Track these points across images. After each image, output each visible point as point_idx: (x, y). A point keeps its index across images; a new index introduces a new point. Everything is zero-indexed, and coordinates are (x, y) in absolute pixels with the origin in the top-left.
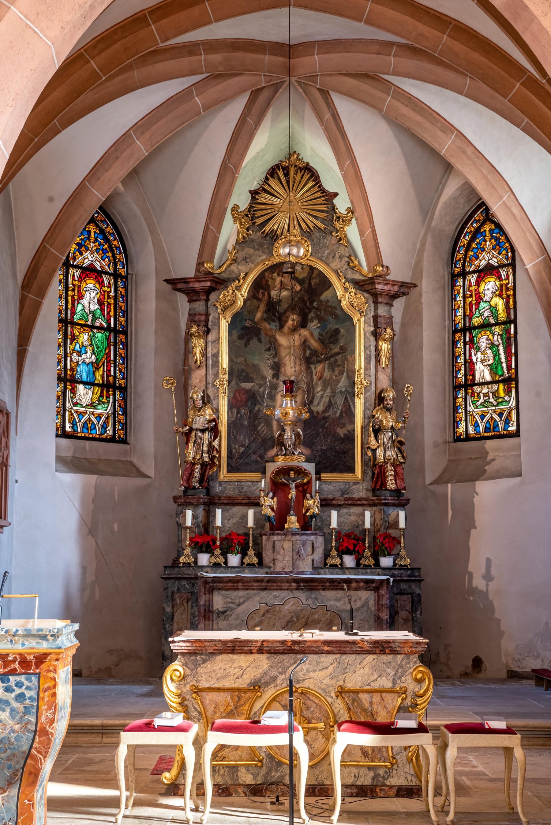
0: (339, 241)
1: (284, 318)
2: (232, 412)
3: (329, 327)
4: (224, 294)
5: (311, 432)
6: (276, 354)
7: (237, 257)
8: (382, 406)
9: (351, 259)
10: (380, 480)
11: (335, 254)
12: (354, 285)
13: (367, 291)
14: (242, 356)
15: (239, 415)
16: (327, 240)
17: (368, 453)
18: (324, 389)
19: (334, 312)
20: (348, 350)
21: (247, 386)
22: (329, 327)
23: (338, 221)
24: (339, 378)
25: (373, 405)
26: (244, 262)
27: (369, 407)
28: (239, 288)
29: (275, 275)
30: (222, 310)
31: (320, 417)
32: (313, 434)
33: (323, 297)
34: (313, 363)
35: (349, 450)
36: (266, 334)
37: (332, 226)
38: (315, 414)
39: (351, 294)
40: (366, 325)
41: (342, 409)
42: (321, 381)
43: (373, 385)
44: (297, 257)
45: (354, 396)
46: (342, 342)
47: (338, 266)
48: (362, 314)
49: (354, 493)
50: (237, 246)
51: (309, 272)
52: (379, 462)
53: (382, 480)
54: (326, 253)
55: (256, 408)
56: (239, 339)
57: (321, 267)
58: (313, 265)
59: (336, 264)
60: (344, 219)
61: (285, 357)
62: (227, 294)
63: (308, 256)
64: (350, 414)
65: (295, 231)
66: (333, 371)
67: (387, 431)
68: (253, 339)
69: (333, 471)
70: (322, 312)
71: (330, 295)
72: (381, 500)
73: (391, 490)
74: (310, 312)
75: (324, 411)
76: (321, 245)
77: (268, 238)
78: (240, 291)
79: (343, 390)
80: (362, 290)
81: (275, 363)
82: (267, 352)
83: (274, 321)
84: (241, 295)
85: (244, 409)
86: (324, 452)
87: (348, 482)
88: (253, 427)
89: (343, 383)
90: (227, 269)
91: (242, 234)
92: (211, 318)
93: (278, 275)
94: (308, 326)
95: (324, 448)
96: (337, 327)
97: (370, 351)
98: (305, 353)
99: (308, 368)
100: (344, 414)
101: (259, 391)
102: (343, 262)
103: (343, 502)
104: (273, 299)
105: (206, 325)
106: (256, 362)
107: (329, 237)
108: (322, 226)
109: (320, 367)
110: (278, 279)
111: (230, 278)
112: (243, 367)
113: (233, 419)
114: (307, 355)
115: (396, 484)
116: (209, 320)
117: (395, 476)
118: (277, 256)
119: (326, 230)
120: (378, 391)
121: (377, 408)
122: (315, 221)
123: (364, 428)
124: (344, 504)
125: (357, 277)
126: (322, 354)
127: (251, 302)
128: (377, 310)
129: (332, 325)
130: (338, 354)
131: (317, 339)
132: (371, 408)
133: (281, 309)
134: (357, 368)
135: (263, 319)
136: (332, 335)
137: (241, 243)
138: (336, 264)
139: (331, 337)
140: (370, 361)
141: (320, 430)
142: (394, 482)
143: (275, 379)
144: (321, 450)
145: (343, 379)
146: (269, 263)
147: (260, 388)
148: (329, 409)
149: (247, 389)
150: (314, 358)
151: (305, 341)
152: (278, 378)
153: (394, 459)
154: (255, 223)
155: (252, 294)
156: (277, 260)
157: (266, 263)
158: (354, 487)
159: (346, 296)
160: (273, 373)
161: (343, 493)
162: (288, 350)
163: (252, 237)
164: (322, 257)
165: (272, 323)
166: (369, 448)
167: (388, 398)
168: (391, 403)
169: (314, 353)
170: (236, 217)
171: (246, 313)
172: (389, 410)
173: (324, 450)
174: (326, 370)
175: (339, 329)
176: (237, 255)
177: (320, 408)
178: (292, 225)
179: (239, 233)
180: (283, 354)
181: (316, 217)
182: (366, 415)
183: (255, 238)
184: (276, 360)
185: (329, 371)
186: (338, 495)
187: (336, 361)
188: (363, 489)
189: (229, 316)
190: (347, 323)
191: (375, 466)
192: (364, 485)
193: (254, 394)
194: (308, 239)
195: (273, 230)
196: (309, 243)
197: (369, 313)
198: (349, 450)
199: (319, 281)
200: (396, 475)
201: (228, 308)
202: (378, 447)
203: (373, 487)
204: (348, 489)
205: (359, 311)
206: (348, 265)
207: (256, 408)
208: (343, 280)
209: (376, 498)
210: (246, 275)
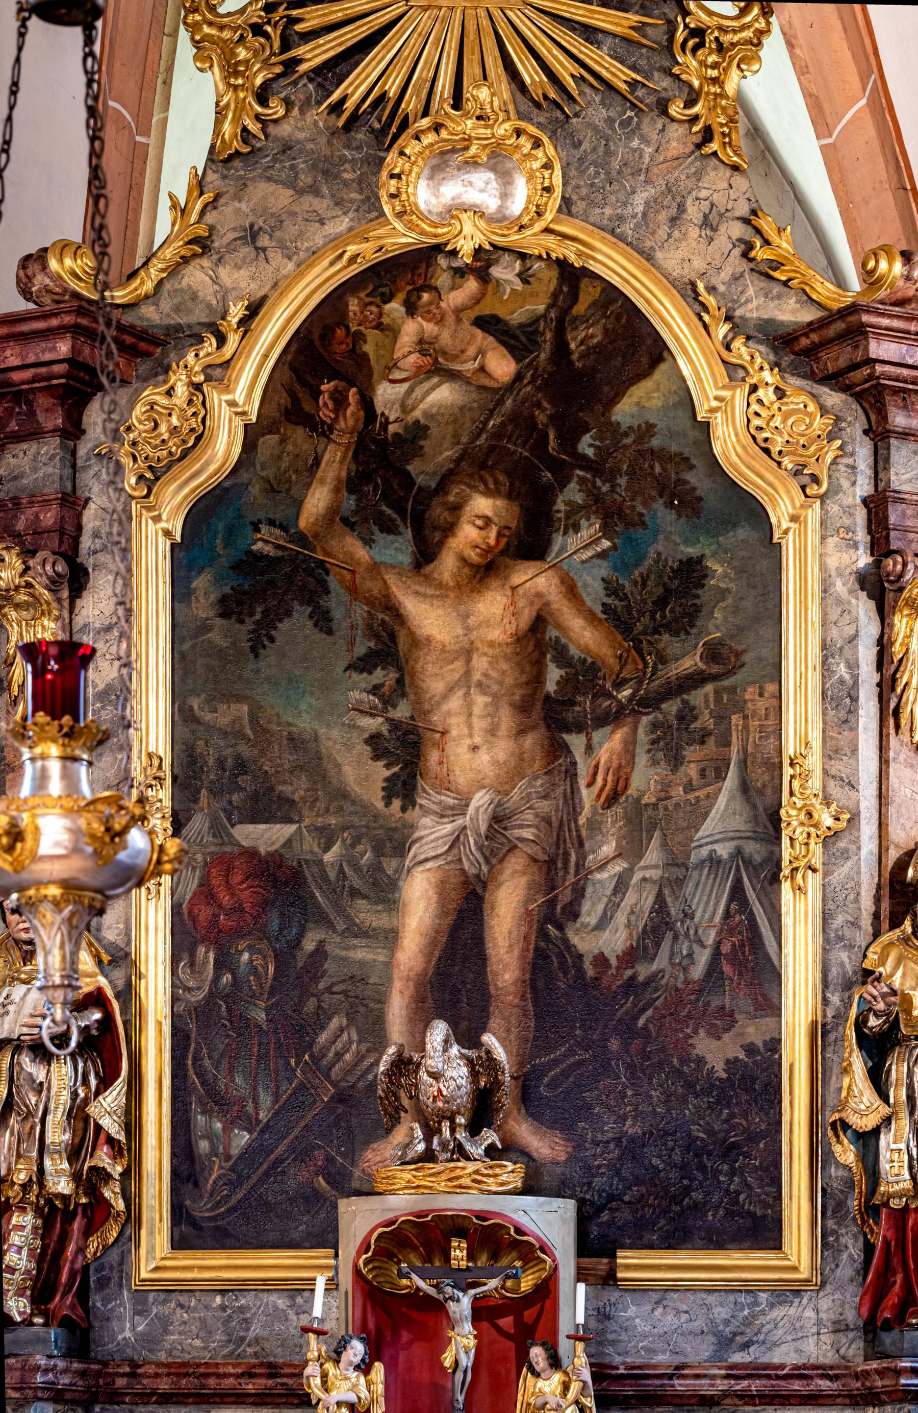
0: (699, 146)
1: (437, 512)
2: (192, 964)
3: (652, 554)
4: (152, 405)
5: (571, 1052)
6: (404, 685)
7: (212, 228)
9: (758, 231)
10: (899, 1278)
11: (681, 208)
12: (775, 350)
13: (834, 380)
14: (239, 698)
15: (227, 978)
16: (645, 140)
17: (837, 1149)
18: (632, 850)
19: (680, 482)
20: (745, 662)
21: (266, 836)
22: (652, 554)
23: (694, 50)
24: (701, 793)
25: (866, 922)
26: (246, 251)
27: (848, 933)
28: (219, 373)
29: (395, 307)
30: (141, 477)
31: (613, 981)
32: (581, 1063)
33: (625, 411)
34: (578, 727)
35: (752, 1137)
36: (353, 590)
37: (668, 72)
38: (590, 971)
39: (761, 393)
40: (832, 542)
41: (718, 944)
42: (618, 809)
43: (868, 830)
44: (499, 219)
45: (775, 880)
46: (716, 625)
47: (699, 264)
48: (813, 490)
49: (776, 1344)
50: (211, 177)
51: (555, 295)
52: (891, 1196)
54: (639, 201)
55: (309, 945)
56: (223, 615)
57: (612, 264)
58: (572, 258)
59: (687, 254)
60: (726, 39)
61: (445, 697)
62: (164, 401)
63: (549, 216)
64: (751, 962)
65: (484, 94)
66: (676, 761)
68: (289, 613)
69: (673, 1241)
70: (622, 481)
71: (656, 402)
72: (898, 1373)
74: (563, 483)
75: (631, 956)
76: (615, 164)
77: (361, 135)
78: (228, 389)
79: (723, 851)
80: (811, 376)
81: (395, 725)
82: (355, 676)
83: (389, 528)
84: (232, 404)
85: (250, 948)
86: (631, 1148)
87: (749, 1289)
88: (296, 1034)
89: (722, 820)
90: (167, 286)
91: (237, 119)
92: (91, 518)
93: (411, 309)
94: (555, 548)
95: (632, 1128)
96: (692, 551)
97: (853, 666)
98: (538, 679)
99: (556, 750)
100: (727, 969)
101: (320, 863)
102: (722, 242)
103: (722, 1385)
104: (387, 422)
105: (69, 551)
106: (304, 723)
107: (651, 126)
108: (618, 74)
109: (610, 744)
110: (410, 329)
111: (178, 328)
112: (244, 750)
113: (200, 995)
114: (551, 686)
116: (79, 528)
118: (400, 215)
119: (640, 93)
120: (893, 855)
121: (885, 938)
122: (586, 52)
123: (822, 1034)
124: (725, 1394)
125: (791, 313)
126: (619, 684)
127: (283, 441)
128: (886, 469)
129: (670, 539)
130: (695, 680)
131: (598, 609)
132: (861, 939)
133: (424, 472)
134: (790, 748)
135: (335, 517)
136: (667, 590)
137: (230, 160)
138: (687, 254)
139: (661, 602)
140: (853, 711)
141: (614, 1045)
143: (397, 804)
144: (618, 1141)
145: (722, 801)
146: (366, 252)
147: (327, 849)
148: (658, 945)
149: (262, 850)
150: (586, 703)
151: (539, 622)
152: (409, 801)
154: (298, 61)
155: (284, 399)
156: (400, 237)
157: (352, 249)
159: (736, 408)
160: (388, 773)
161: (725, 1343)
162: (459, 664)
163: (285, 130)
164: (621, 218)
165: (379, 536)
166: (845, 1126)
169: (584, 675)
170: (206, 38)
171: (255, 490)
173: (633, 1139)
174: (642, 759)
175: (700, 559)
176: (210, 218)
177: (614, 941)
178: (471, 69)
179: (220, 113)
180: (436, 686)
181: (589, 33)
182: (834, 972)
183: (301, 136)
184: (402, 712)
185: (655, 763)
186: (699, 1351)
187: (687, 715)
188: (819, 1323)
189: (174, 502)
190: (742, 533)
191: (871, 1210)
192: (825, 1303)
193: (296, 878)
194: (553, 136)
195: (382, 98)
196: (551, 151)
197: (845, 484)
198: (752, 1137)
199: (606, 332)
201: (169, 467)
203: (865, 1311)
204: (747, 1322)
205: (796, 473)
206: (745, 255)
207: (309, 945)
208: (723, 330)
209: (874, 1365)
210: (254, 310)
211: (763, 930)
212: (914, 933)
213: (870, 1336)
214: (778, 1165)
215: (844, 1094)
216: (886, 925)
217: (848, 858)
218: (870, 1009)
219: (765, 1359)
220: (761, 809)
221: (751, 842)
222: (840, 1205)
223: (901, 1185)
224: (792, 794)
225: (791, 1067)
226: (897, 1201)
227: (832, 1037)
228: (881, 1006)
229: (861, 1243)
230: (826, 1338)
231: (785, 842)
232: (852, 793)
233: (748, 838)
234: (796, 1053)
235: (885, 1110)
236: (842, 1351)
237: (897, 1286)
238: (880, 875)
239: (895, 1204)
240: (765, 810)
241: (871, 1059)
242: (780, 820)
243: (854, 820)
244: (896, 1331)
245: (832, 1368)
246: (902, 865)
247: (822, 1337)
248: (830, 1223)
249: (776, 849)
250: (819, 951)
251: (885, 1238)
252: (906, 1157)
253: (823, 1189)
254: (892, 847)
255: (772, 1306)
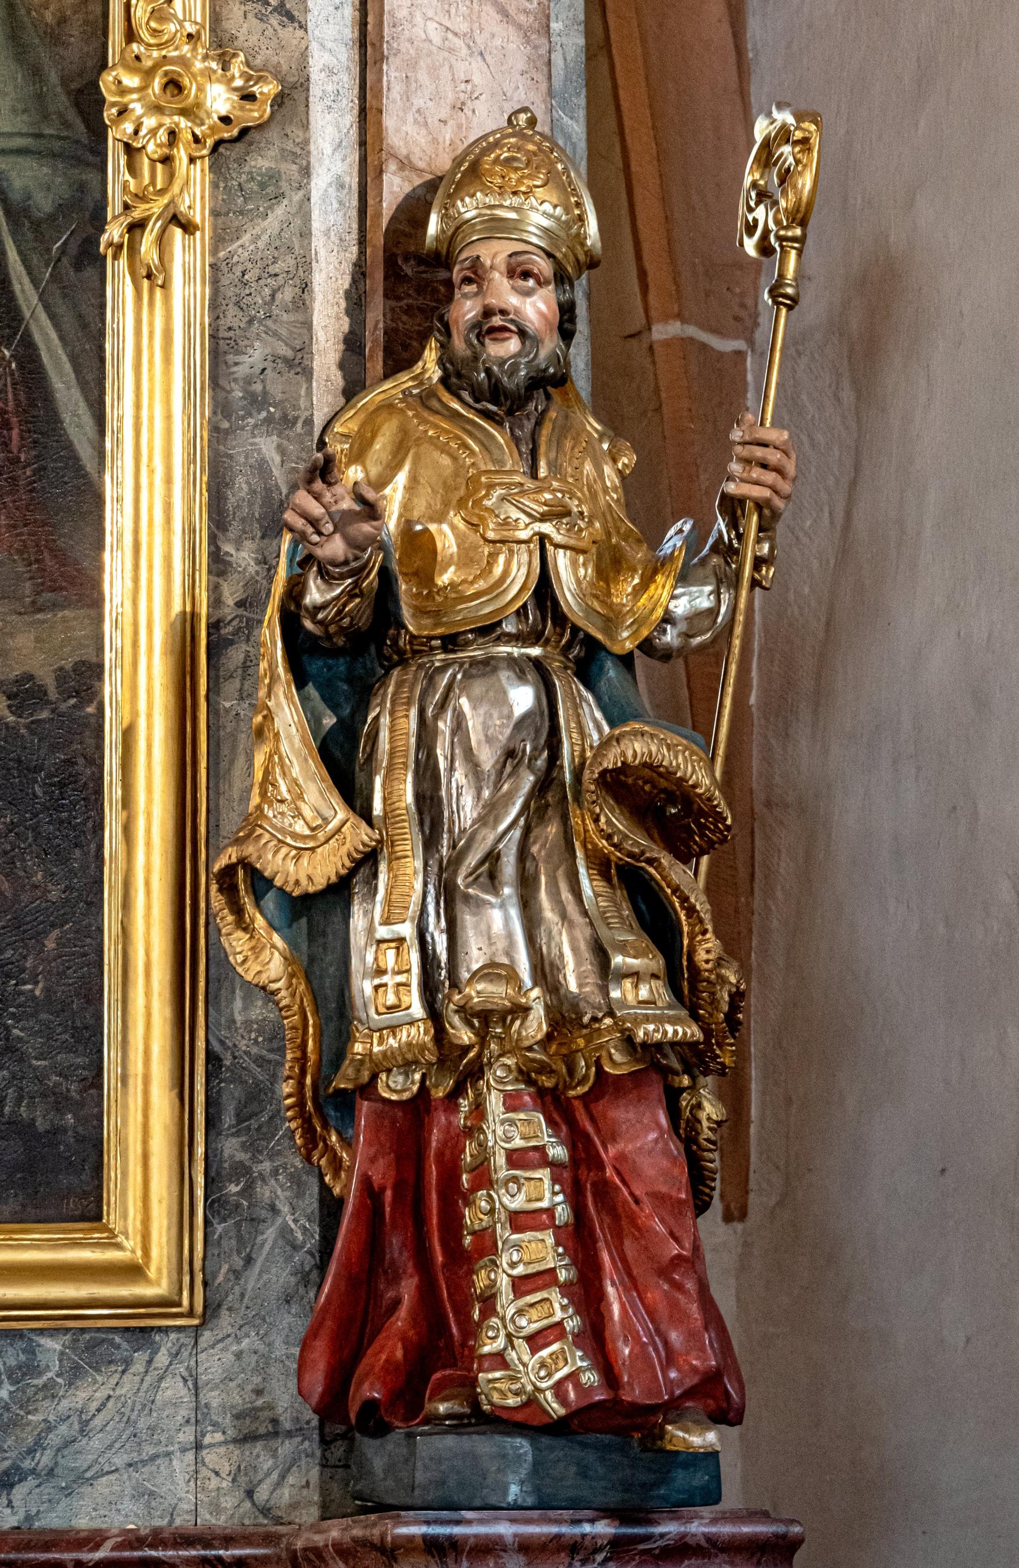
8: (430, 364)
10: (408, 1289)
17: (237, 943)
27: (276, 386)
45: (89, 258)
49: (82, 1479)
52: (380, 1066)
53: (428, 1291)
67: (488, 666)
73: (526, 1422)
115: (595, 1337)
117: (578, 1239)
120: (395, 188)
121: (369, 398)
123: (206, 654)
142: (558, 1308)
153: (564, 1017)
158: (83, 1395)
166: (260, 883)
167: (494, 254)
168: (536, 307)
172: (517, 401)
182: (241, 487)
188: (200, 1416)
191: (331, 1104)
192: (214, 1363)
200: (594, 1212)
202: (367, 862)
203: (317, 1382)
211: (57, 384)
212: (444, 381)
213: (338, 1450)
214: (93, 996)
215: (255, 800)
216: (376, 365)
217: (279, 197)
218: (308, 560)
219: (52, 1520)
220: (53, 77)
221: (28, 163)
222: (257, 1096)
223: (403, 1035)
224: (131, 36)
225: (128, 735)
226: (397, 1080)
227: (235, 656)
228: (336, 548)
229: (311, 1202)
230: (219, 1458)
231: (115, 159)
232: (289, 34)
233: (20, 152)
234: (139, 696)
235: (363, 835)
236: (262, 1494)
237: (403, 1312)
238: (362, 241)
239: (395, 1087)
240: (64, 82)
241: (334, 707)
242: (100, 102)
243: (292, 98)
244: (397, 1436)
245: (228, 1541)
246: (413, 211)
247: (210, 1457)
248: (231, 1147)
249: (90, 177)
250: (203, 434)
251: (366, 1182)
252: (415, 957)
253: (211, 1057)
254: (392, 166)
255: (74, 1374)
